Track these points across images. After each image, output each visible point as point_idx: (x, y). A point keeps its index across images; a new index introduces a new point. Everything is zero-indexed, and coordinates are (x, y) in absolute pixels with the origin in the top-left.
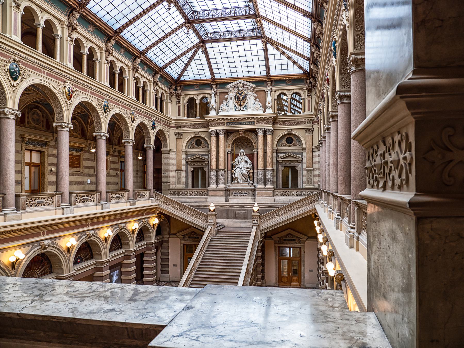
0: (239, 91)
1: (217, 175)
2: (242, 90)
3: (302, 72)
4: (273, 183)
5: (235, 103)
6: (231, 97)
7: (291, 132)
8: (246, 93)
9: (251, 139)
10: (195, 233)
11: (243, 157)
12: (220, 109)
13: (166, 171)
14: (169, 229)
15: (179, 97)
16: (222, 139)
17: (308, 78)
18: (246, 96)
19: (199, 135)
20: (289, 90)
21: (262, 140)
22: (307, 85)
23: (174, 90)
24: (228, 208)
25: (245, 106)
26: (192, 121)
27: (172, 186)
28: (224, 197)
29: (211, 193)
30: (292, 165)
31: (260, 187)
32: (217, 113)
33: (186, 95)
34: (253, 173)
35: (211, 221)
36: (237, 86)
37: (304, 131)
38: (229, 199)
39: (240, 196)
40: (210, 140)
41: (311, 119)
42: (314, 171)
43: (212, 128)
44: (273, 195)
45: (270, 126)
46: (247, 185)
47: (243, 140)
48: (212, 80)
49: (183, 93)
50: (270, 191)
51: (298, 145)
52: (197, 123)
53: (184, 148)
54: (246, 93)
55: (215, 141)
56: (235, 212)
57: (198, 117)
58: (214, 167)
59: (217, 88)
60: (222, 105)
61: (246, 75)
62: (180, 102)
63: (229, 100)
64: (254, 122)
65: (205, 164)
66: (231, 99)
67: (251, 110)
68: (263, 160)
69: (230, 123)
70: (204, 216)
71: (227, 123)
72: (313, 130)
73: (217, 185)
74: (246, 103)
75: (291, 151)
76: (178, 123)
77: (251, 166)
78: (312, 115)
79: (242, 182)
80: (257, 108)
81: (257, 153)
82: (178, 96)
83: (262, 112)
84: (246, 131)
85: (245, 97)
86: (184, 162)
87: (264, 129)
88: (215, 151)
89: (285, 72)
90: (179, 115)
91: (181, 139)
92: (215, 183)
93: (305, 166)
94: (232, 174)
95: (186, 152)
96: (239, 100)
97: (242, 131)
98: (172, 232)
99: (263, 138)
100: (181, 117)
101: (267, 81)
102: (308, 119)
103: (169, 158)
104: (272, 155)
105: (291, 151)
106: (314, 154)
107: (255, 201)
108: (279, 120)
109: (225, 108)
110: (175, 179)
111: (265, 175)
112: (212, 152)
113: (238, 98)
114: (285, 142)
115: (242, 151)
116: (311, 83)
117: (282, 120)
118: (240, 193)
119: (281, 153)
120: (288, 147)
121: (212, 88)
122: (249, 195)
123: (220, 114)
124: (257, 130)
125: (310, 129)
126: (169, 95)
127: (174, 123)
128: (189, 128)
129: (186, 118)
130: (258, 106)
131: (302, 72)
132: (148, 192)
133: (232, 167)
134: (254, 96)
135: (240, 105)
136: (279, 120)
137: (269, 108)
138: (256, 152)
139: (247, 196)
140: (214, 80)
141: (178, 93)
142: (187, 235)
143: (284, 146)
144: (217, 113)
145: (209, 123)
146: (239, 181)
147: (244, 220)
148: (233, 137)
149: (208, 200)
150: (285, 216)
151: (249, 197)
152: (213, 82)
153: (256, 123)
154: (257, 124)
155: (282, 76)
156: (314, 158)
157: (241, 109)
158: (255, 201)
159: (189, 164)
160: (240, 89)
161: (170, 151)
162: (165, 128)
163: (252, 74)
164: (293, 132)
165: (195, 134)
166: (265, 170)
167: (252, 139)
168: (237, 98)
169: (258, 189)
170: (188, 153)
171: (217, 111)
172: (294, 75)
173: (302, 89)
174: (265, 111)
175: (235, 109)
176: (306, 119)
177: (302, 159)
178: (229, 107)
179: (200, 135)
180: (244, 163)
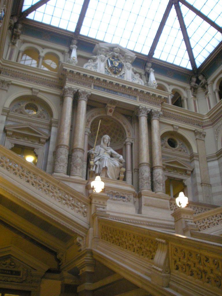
3: (190, 67)
5: (106, 67)
9: (122, 123)
15: (15, 38)
16: (83, 105)
25: (121, 76)
34: (125, 173)
37: (193, 134)
39: (114, 200)
41: (201, 121)
42: (213, 188)
45: (156, 108)
49: (23, 37)
50: (165, 201)
53: (7, 105)
62: (15, 43)
63: (98, 61)
65: (40, 142)
66: (102, 61)
71: (94, 86)
73: (69, 173)
78: (203, 116)
85: (121, 66)
87: (150, 110)
89: (170, 61)
91: (5, 92)
93: (199, 180)
95: (8, 112)
96: (114, 67)
106: (210, 164)
107: (141, 213)
113: (112, 62)
116: (198, 81)
122: (129, 201)
124: (140, 107)
125: (200, 133)
131: (190, 67)
138: (130, 143)
143: (166, 147)
146: (109, 176)
148: (96, 114)
153: (138, 99)
160: (116, 54)
164: (180, 131)
167: (125, 124)
173: (184, 88)
179: (40, 96)
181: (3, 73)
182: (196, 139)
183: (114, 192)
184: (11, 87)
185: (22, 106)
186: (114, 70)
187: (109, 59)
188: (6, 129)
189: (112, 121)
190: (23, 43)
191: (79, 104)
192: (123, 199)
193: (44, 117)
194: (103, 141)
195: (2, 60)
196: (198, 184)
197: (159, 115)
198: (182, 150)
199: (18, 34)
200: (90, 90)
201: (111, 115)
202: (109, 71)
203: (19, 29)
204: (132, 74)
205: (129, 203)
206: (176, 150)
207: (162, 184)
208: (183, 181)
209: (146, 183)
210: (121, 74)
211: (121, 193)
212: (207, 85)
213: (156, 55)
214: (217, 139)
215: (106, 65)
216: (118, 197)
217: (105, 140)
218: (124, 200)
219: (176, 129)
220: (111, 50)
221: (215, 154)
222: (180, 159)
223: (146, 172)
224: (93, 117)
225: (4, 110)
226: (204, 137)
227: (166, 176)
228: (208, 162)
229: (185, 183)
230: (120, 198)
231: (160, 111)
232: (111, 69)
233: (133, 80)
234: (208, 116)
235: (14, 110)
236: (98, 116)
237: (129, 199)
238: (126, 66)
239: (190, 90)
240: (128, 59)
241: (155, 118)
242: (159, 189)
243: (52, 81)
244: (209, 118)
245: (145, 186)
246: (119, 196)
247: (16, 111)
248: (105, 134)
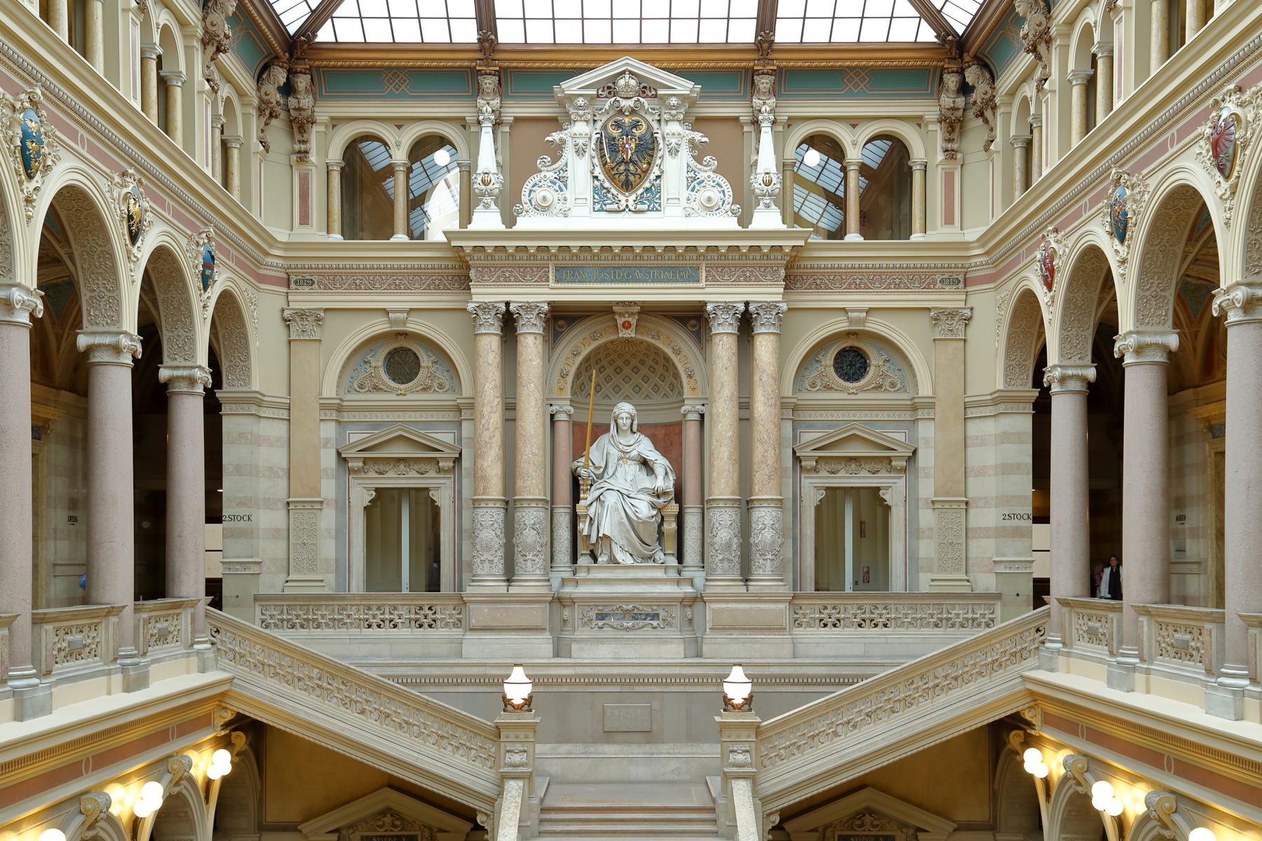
0: (621, 112)
1: (510, 529)
2: (633, 112)
3: (928, 35)
4: (780, 569)
5: (598, 171)
6: (581, 142)
7: (864, 321)
8: (655, 125)
9: (669, 352)
10: (395, 815)
11: (631, 439)
12: (525, 199)
13: (241, 503)
14: (261, 802)
15: (302, 129)
16: (531, 345)
17: (954, 67)
18: (654, 140)
19: (412, 327)
20: (854, 122)
21: (734, 359)
22: (947, 100)
23: (280, 89)
25: (647, 190)
26: (368, 250)
27: (271, 583)
28: (547, 635)
29: (478, 614)
30: (863, 479)
31: (724, 582)
32: (510, 220)
33: (335, 122)
35: (517, 758)
36: (609, 87)
38: (574, 647)
40: (473, 356)
41: (959, 263)
42: (972, 512)
43: (488, 294)
44: (786, 621)
45: (767, 293)
46: (659, 574)
47: (620, 356)
48: (481, 51)
49: (324, 112)
50: (772, 606)
51: (893, 385)
52: (409, 263)
53: (329, 391)
54: (655, 125)
55: (498, 359)
57: (400, 237)
58: (495, 490)
59: (502, 90)
60: (535, 179)
61: (655, 34)
62: (306, 152)
63: (569, 154)
64: (698, 268)
65: (439, 470)
66: (580, 152)
67: (679, 211)
68: (735, 457)
69: (574, 268)
70: (474, 729)
71: (557, 269)
72: (969, 319)
73: (510, 576)
74: (652, 177)
75: (859, 416)
76: (300, 263)
77: (669, 485)
78: (966, 245)
79: (629, 561)
80: (709, 199)
82: (299, 126)
83: (731, 224)
84: (649, 311)
85: (648, 148)
86: (328, 459)
87: (742, 307)
88: (500, 407)
90: (305, 220)
91: (314, 345)
92: (499, 568)
93: (926, 488)
94: (575, 519)
95: (339, 409)
96: (623, 161)
97: (631, 314)
98: (272, 816)
99: (735, 349)
100: (314, 233)
101: (754, 72)
102: (946, 263)
103: (258, 441)
104: (779, 428)
105: (859, 416)
106: (974, 428)
108: (809, 263)
109: (551, 194)
110: (283, 544)
111: (745, 529)
112: (486, 411)
115: (625, 409)
116: (965, 89)
117: (829, 263)
118: (626, 614)
119: (811, 425)
120: (845, 393)
121: (478, 91)
122: (670, 624)
123: (523, 224)
124: (709, 308)
125: (951, 314)
126: (254, 112)
127: (280, 262)
128: (358, 287)
129: (337, 237)
130: (715, 194)
131: (928, 35)
132: (186, 616)
134: (692, 142)
135: (627, 186)
136: (809, 263)
137: (767, 206)
138: (695, 417)
140: (494, 51)
141: (299, 109)
142: (352, 826)
143: (828, 388)
144: (510, 220)
145: (469, 268)
147: (647, 748)
148: (580, 343)
149: (466, 650)
150: (882, 726)
151: (671, 633)
152: (487, 61)
154: (711, 279)
155: (830, 48)
156: (970, 450)
157: (631, 203)
158: (699, 655)
159: (351, 471)
161: (259, 403)
162: (243, 285)
163: (684, 34)
164: (876, 325)
165: (391, 322)
166: (746, 505)
167: (677, 352)
168: (609, 150)
169: (715, 595)
170: (347, 417)
171: (509, 207)
172: (887, 48)
174: (744, 220)
175: (601, 200)
176: (939, 263)
177: (915, 452)
178: (567, 193)
179: (416, 325)
180: (633, 469)
181: (296, 282)
184: (331, 322)
185: (373, 364)
186: (623, 177)
187: (605, 127)
188: (343, 456)
190: (334, 126)
191: (520, 348)
192: (651, 622)
193: (441, 386)
194: (616, 421)
195: (280, 246)
197: (774, 313)
199: (305, 114)
200: (547, 290)
201: (633, 336)
202: (607, 185)
203: (303, 93)
204: (688, 166)
206: (862, 390)
207: (770, 557)
208: (881, 492)
210: (647, 185)
211: (646, 605)
212: (994, 108)
213: (785, 33)
215: (596, 161)
216: (637, 619)
217: (620, 422)
218: (655, 623)
220: (609, 88)
221: (989, 397)
223: (724, 524)
224: (579, 354)
225: (324, 407)
226: (966, 325)
230: (645, 619)
231: (779, 298)
232: (611, 174)
233: (693, 190)
234: (983, 246)
235: (356, 386)
236: (595, 345)
237: (669, 619)
238: (664, 138)
239: (937, 127)
240: (672, 107)
241: (763, 330)
242: (761, 572)
243: (440, 268)
244: (987, 253)
245: (719, 571)
246: (640, 614)
247: (361, 386)
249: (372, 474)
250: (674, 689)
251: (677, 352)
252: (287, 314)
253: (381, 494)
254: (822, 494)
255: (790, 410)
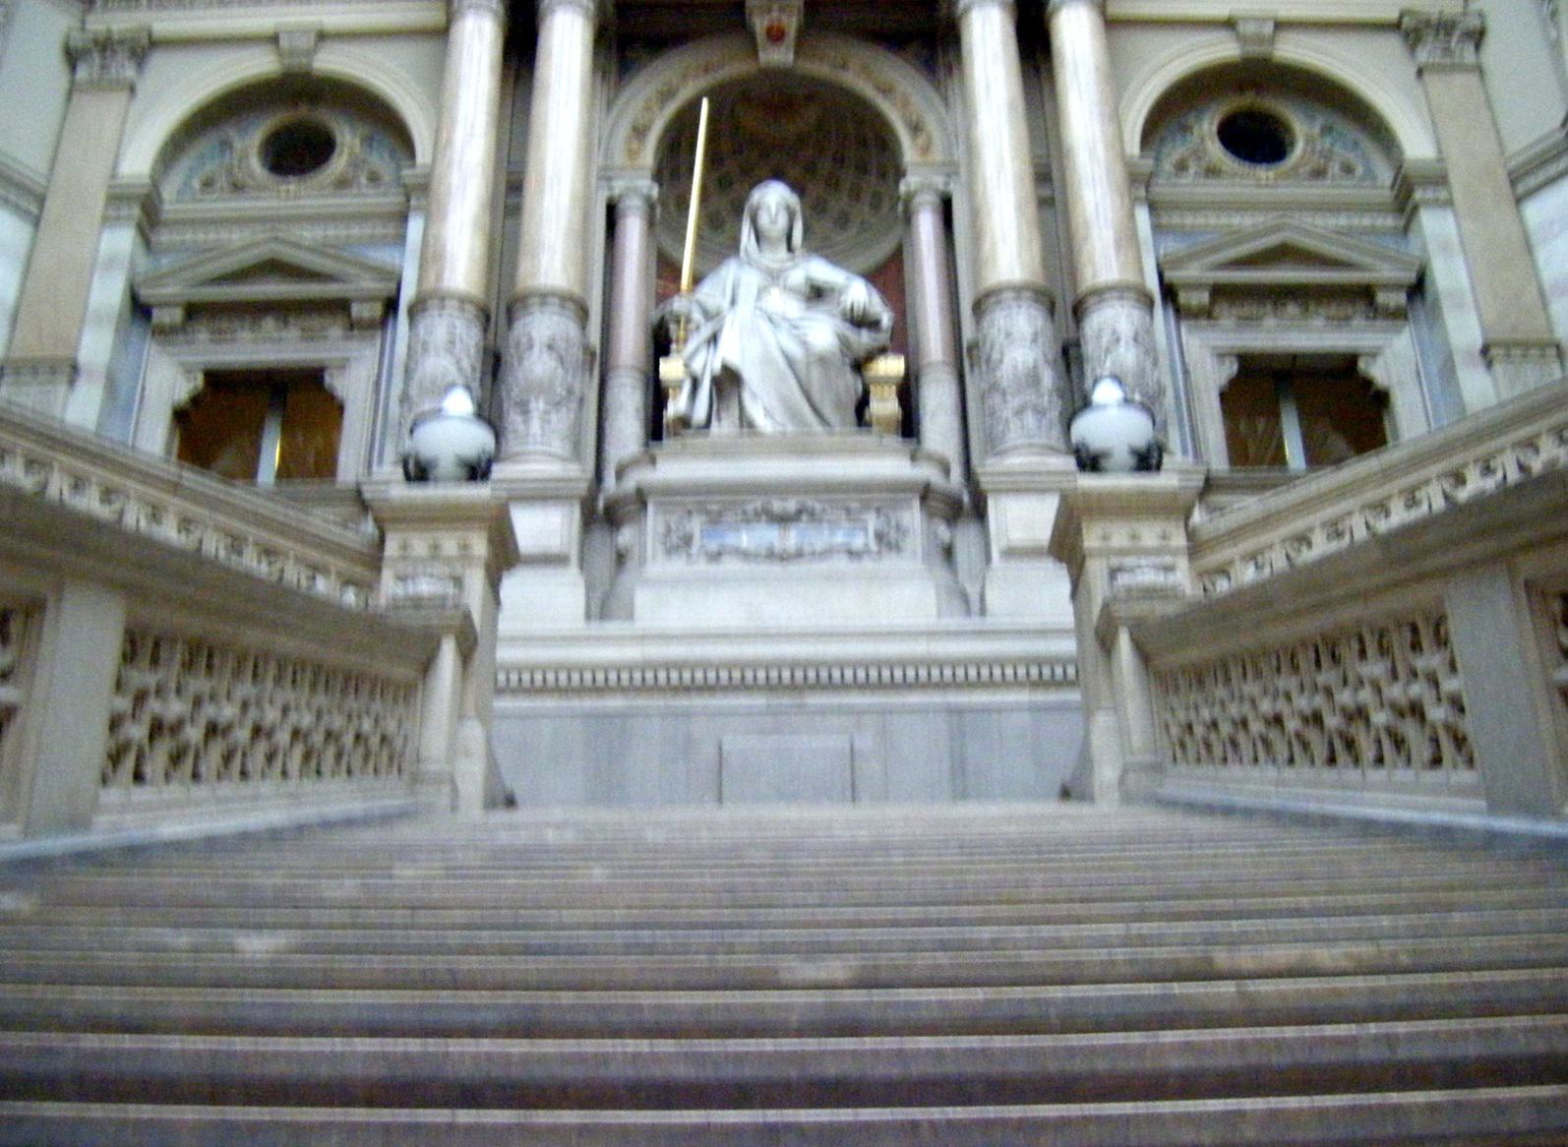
9: (868, 90)
24: (615, 703)
34: (907, 392)
37: (1393, 44)
38: (643, 599)
51: (1348, 170)
56: (708, 751)
65: (352, 325)
81: (946, 210)
86: (109, 293)
93: (1464, 330)
94: (657, 394)
114: (1216, 150)
115: (773, 199)
119: (1183, 232)
122: (895, 547)
133: (660, 342)
139: (868, 564)
143: (1212, 172)
156: (1541, 255)
167: (886, 91)
179: (332, 62)
182: (1420, 72)
183: (777, 506)
184: (158, 61)
185: (238, 145)
189: (810, 98)
196: (1457, 358)
198: (1334, 168)
205: (890, 563)
208: (1362, 365)
209: (1019, 412)
214: (1554, 33)
217: (764, 220)
219: (1260, 39)
222: (1315, 230)
225: (117, 197)
227: (1221, 356)
228: (1519, 201)
229: (1378, 372)
235: (196, 184)
247: (208, 184)
248: (753, 178)
249: (203, 335)
250: (914, 699)
251: (886, 91)
252: (78, 41)
253: (219, 382)
254: (1231, 368)
255: (1139, 184)
